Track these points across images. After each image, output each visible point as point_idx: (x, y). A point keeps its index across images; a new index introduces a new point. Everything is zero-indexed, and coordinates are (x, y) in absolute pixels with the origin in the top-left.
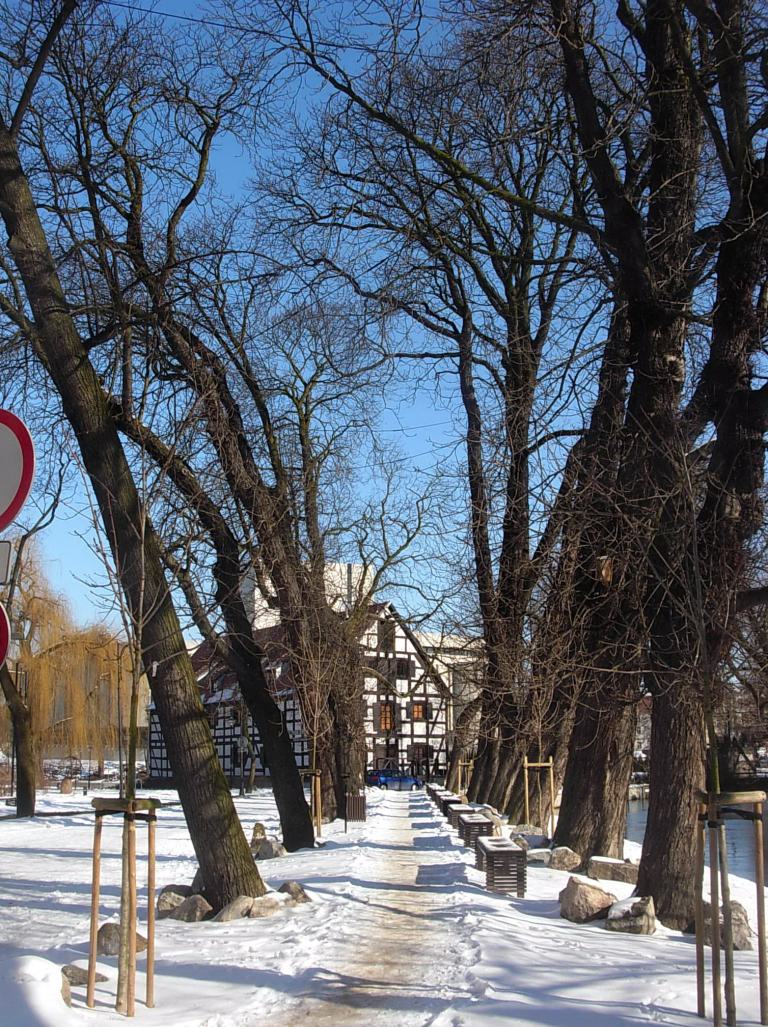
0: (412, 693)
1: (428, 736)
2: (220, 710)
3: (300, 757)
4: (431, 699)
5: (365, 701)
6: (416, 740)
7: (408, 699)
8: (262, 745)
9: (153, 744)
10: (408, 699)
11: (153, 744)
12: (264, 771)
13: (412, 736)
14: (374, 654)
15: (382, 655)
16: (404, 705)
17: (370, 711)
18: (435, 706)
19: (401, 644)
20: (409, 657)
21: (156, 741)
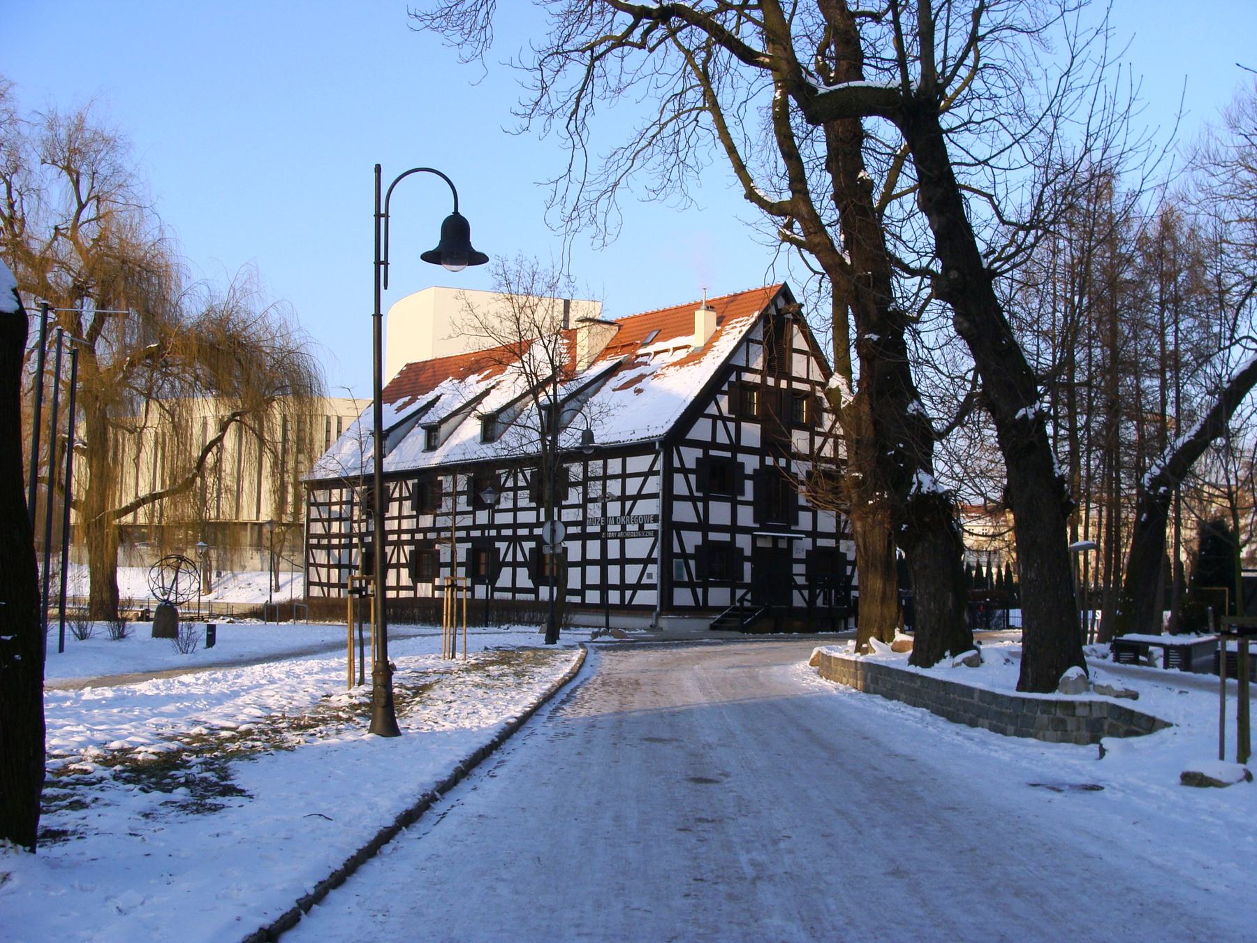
0: (814, 456)
1: (838, 535)
2: (446, 482)
3: (618, 568)
5: (742, 464)
7: (808, 465)
8: (533, 544)
9: (314, 541)
10: (808, 465)
11: (314, 541)
12: (535, 591)
13: (814, 534)
14: (757, 379)
15: (771, 381)
16: (802, 477)
17: (749, 485)
19: (799, 365)
20: (813, 389)
21: (319, 537)
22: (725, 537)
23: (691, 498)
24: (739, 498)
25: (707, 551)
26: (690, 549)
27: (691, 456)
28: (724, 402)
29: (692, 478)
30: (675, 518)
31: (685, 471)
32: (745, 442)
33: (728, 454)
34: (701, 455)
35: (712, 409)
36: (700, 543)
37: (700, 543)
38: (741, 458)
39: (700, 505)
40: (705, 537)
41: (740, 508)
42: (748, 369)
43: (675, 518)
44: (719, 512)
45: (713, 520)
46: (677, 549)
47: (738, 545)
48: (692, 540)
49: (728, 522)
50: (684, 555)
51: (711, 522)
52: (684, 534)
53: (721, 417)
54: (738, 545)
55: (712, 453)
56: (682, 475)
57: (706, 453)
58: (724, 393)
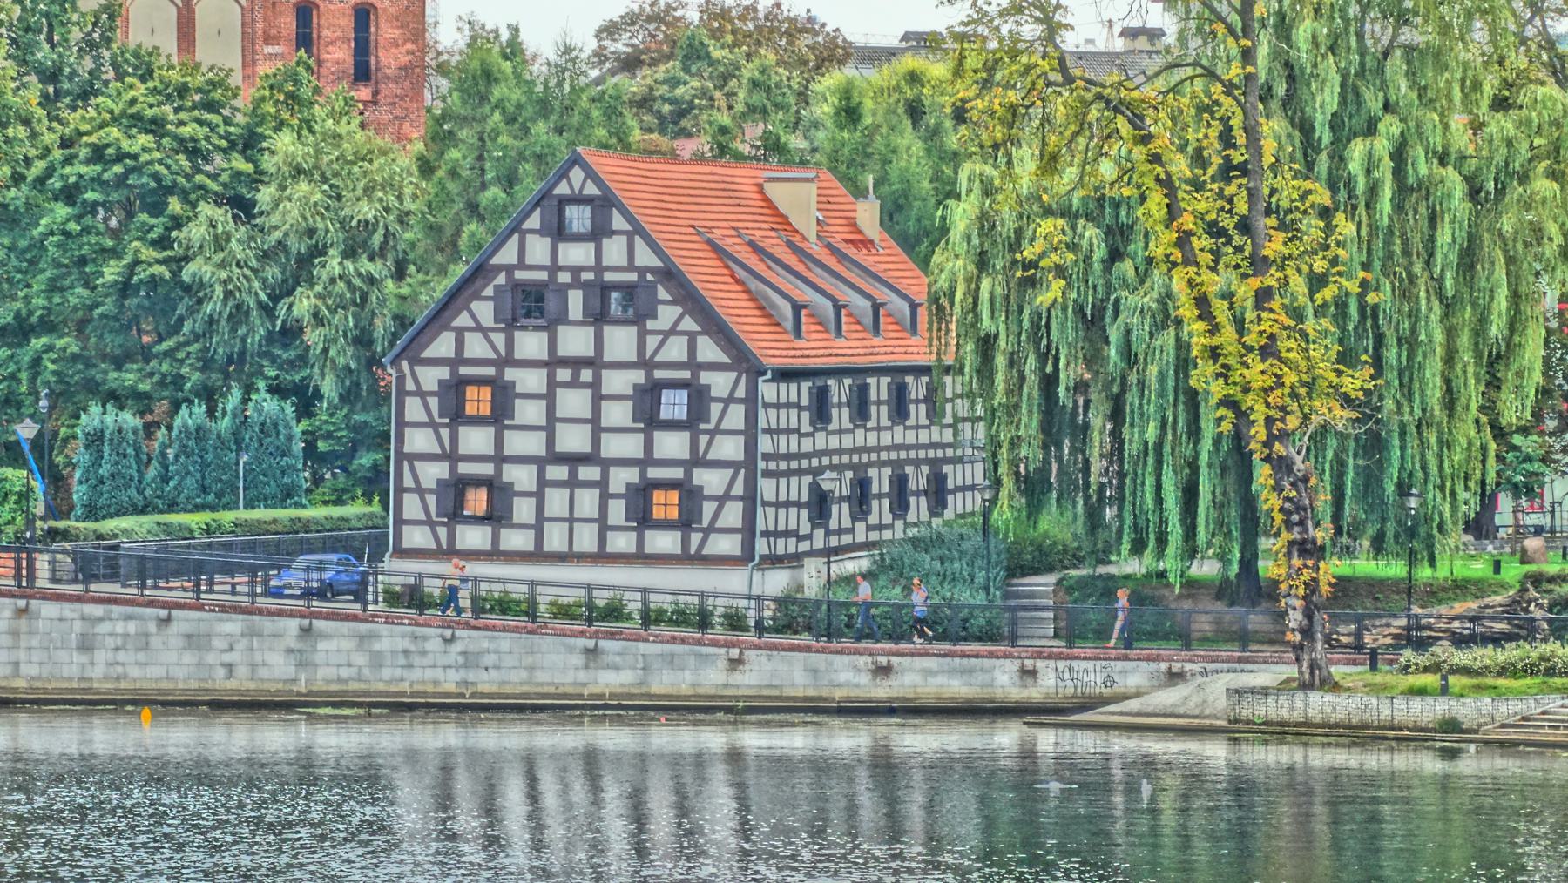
4: (706, 377)
6: (654, 473)
18: (713, 394)
22: (487, 469)
23: (432, 425)
24: (507, 422)
25: (456, 488)
26: (428, 482)
27: (431, 377)
28: (484, 311)
29: (434, 402)
30: (407, 449)
31: (421, 394)
32: (517, 356)
33: (490, 371)
34: (447, 376)
35: (463, 320)
36: (446, 476)
37: (446, 476)
38: (510, 374)
39: (445, 433)
40: (453, 469)
41: (506, 433)
42: (522, 265)
43: (407, 449)
44: (476, 440)
45: (462, 450)
46: (408, 482)
47: (505, 478)
48: (433, 472)
49: (490, 450)
50: (419, 490)
51: (462, 450)
52: (416, 463)
53: (479, 328)
54: (505, 478)
55: (464, 371)
56: (418, 399)
57: (454, 373)
58: (487, 298)
